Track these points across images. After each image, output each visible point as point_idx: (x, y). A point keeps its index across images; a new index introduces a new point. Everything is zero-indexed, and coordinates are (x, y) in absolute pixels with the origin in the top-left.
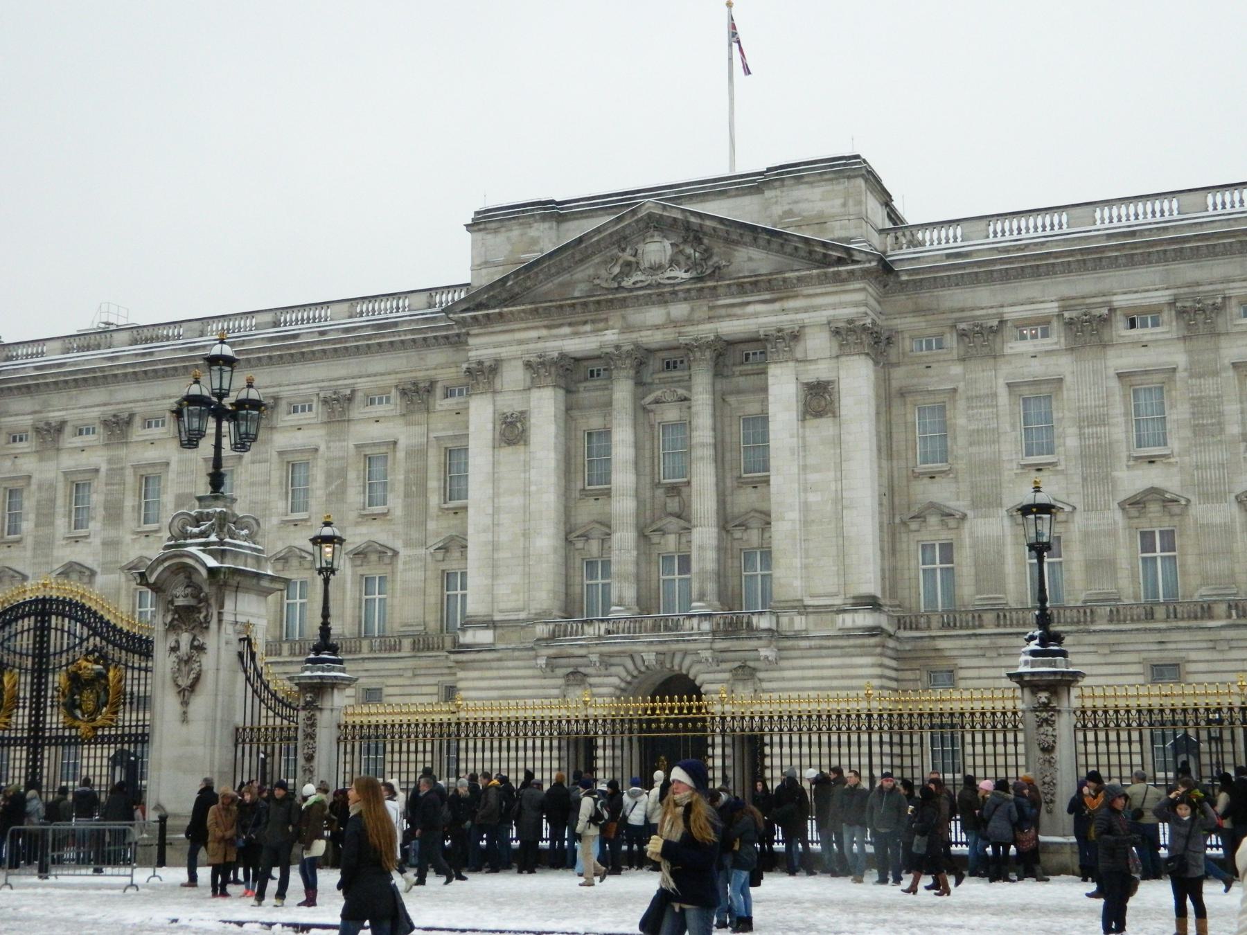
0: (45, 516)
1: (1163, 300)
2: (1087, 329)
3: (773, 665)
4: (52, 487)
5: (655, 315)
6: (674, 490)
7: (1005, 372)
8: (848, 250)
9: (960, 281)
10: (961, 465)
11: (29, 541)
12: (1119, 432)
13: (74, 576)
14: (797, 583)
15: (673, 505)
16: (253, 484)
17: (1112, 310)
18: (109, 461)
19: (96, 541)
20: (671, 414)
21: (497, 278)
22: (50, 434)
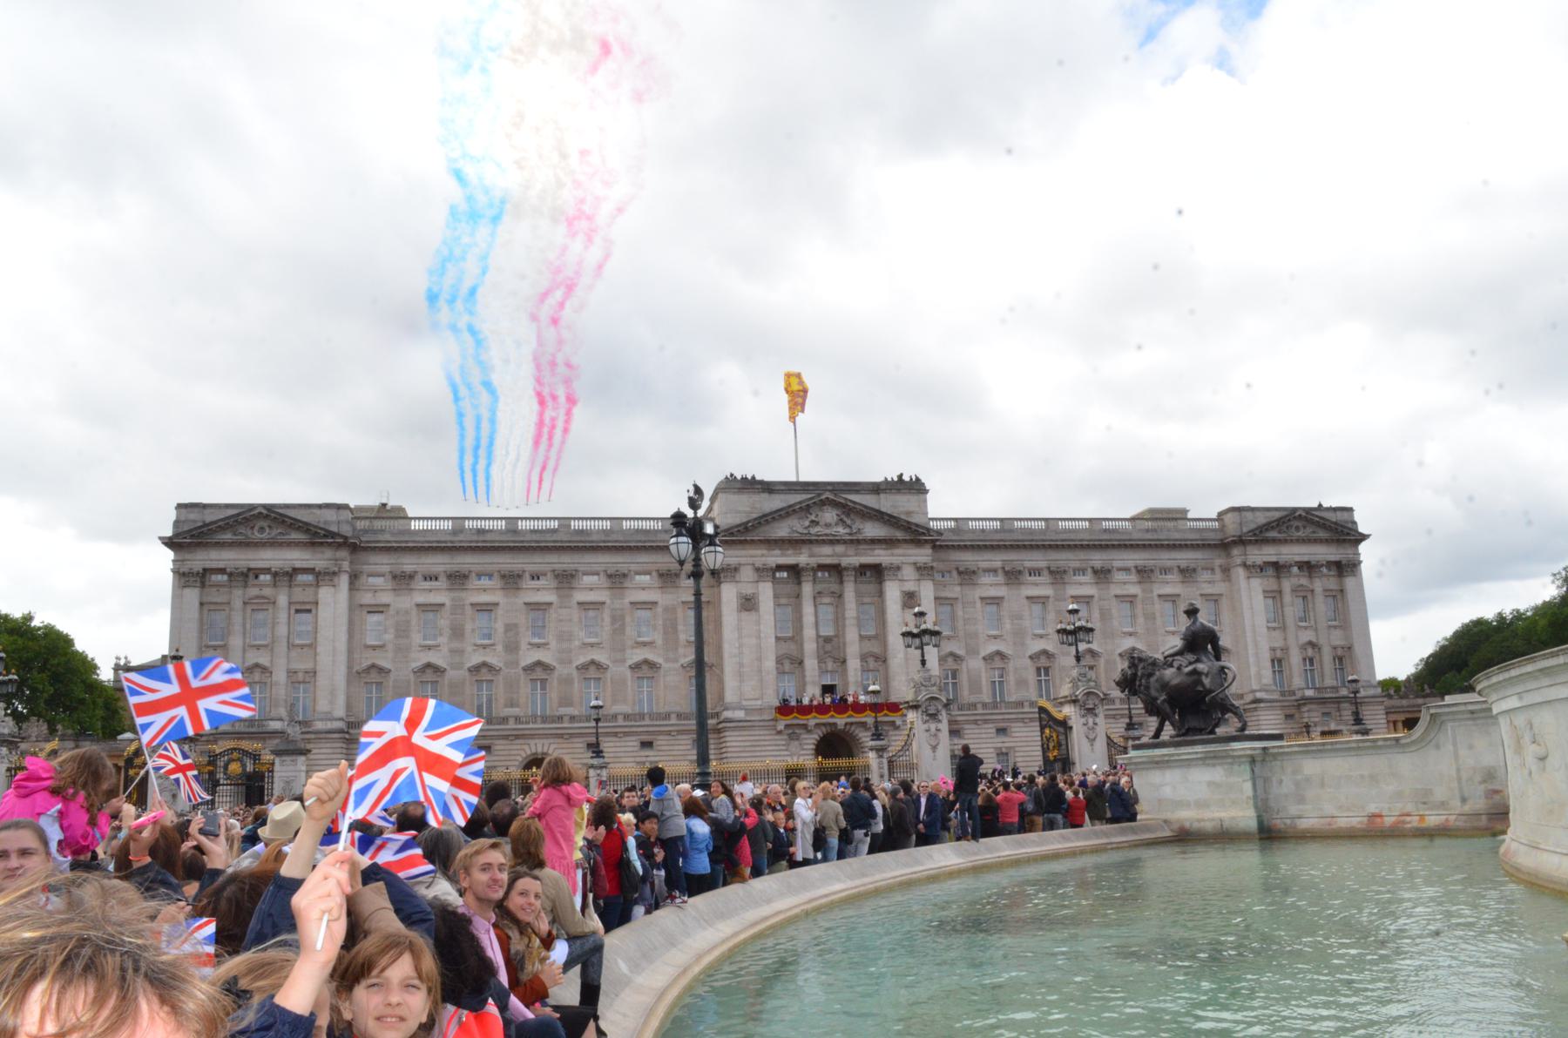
0: (402, 631)
2: (1013, 576)
3: (898, 728)
4: (407, 612)
5: (827, 550)
6: (828, 640)
7: (979, 592)
8: (928, 530)
9: (960, 548)
10: (961, 633)
13: (429, 671)
15: (828, 647)
19: (445, 650)
20: (827, 600)
21: (738, 521)
22: (403, 580)
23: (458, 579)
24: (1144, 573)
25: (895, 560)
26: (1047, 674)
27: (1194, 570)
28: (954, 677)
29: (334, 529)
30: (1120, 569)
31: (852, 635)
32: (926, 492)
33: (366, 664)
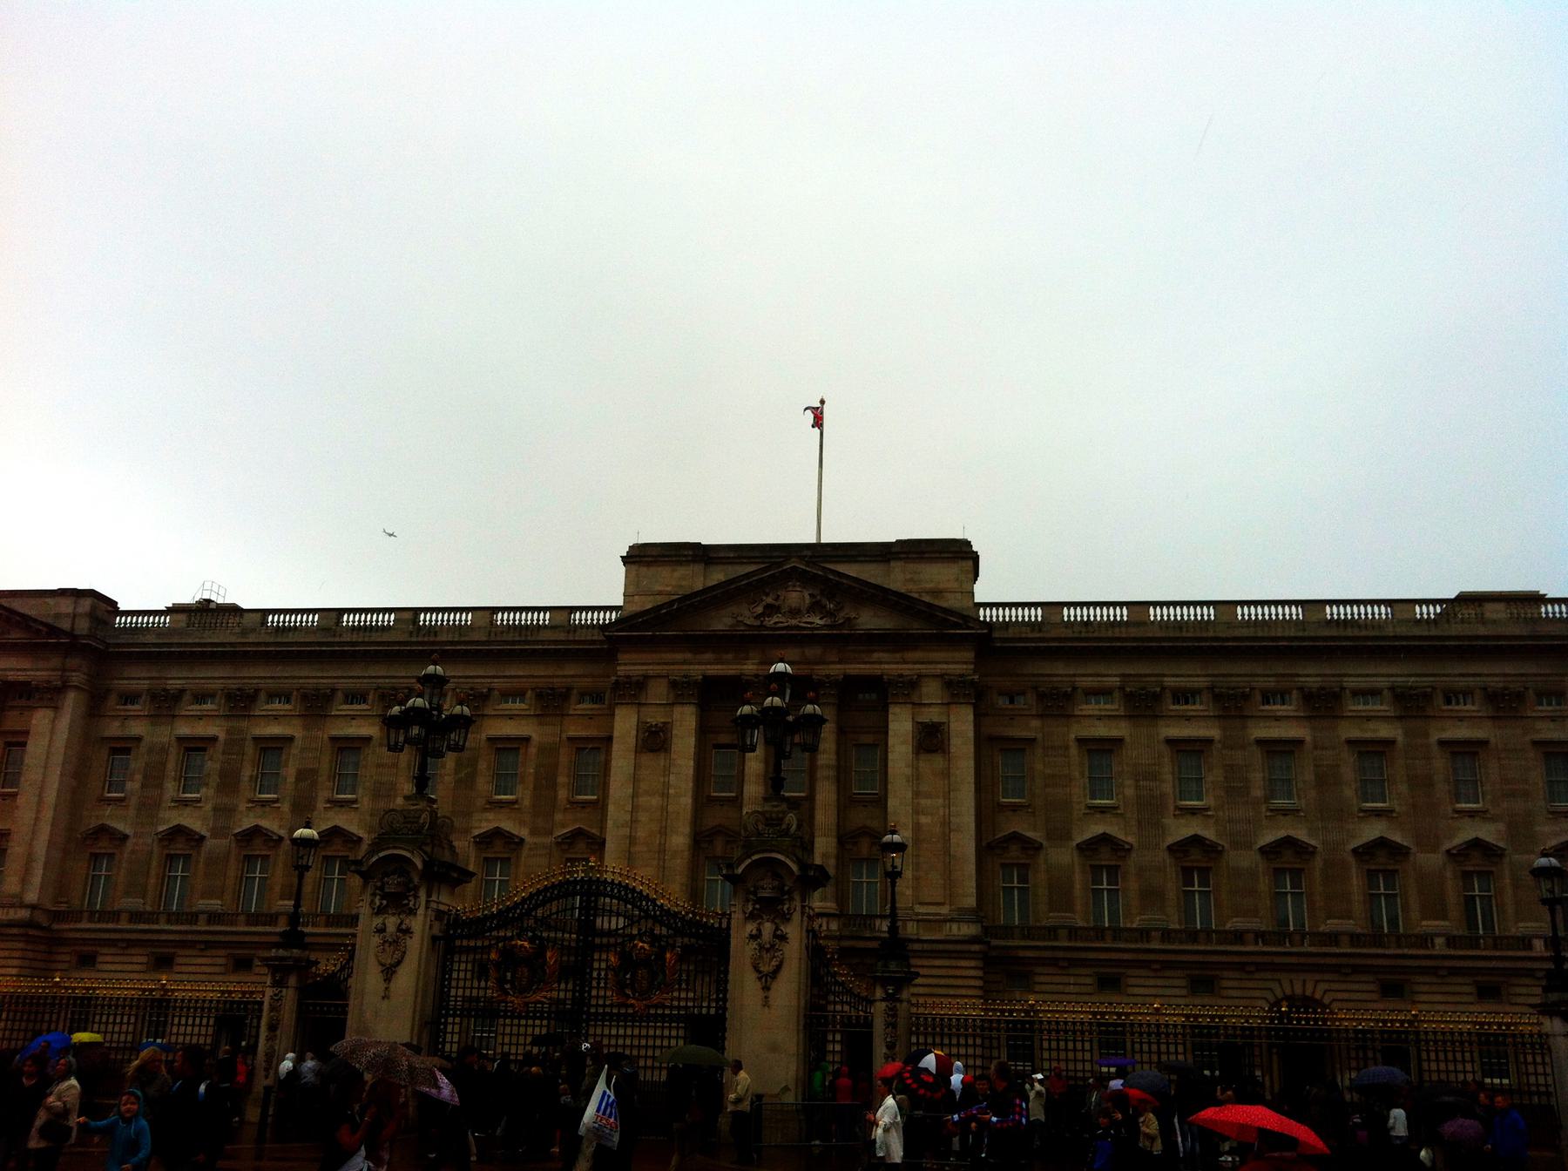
0: (153, 778)
1: (1202, 685)
2: (1143, 705)
4: (164, 750)
11: (134, 801)
12: (1168, 788)
14: (909, 892)
16: (379, 766)
17: (1163, 689)
18: (228, 732)
19: (208, 807)
22: (165, 704)
23: (241, 702)
24: (1411, 704)
25: (907, 670)
26: (1204, 882)
27: (1519, 697)
28: (1023, 879)
29: (65, 625)
30: (1358, 693)
31: (826, 794)
32: (975, 558)
33: (94, 823)
